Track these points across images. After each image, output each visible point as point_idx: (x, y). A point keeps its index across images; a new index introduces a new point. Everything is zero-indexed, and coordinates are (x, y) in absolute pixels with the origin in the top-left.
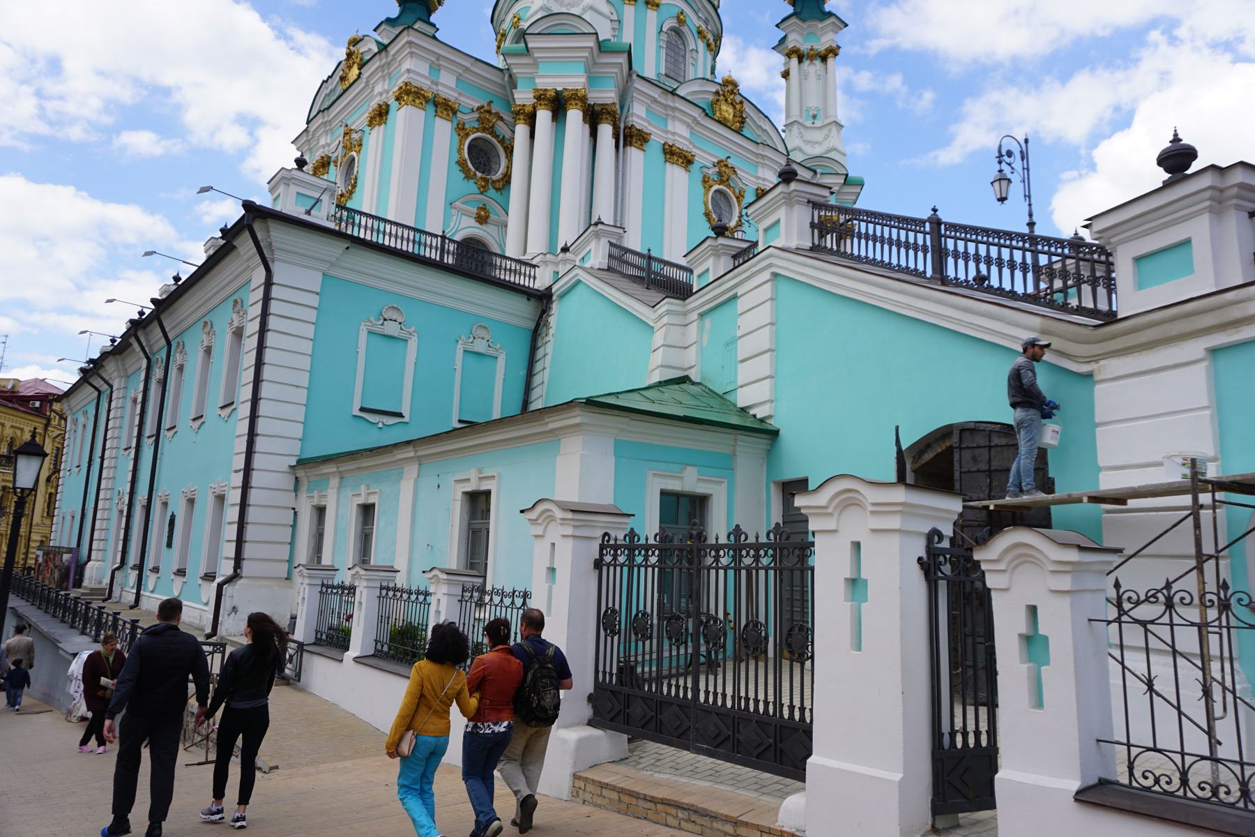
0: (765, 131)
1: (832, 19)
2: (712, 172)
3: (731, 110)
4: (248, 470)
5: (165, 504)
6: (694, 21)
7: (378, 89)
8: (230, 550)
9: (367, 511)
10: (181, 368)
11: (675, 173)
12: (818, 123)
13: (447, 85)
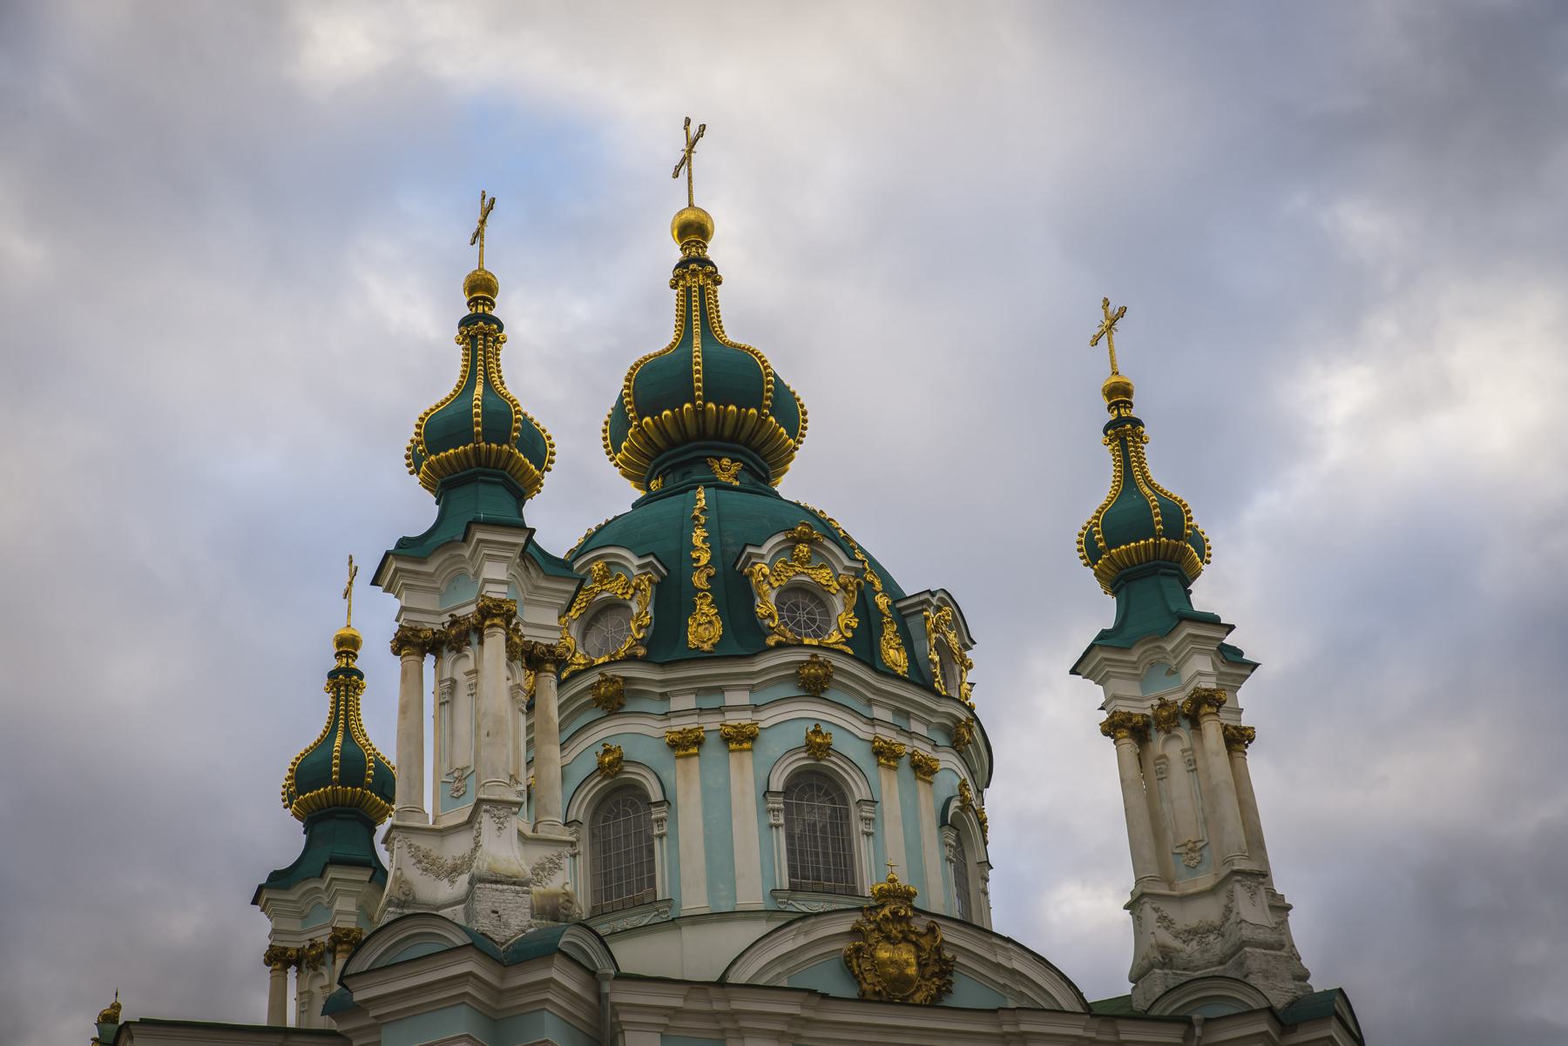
0: (1013, 972)
1: (1188, 629)
3: (906, 954)
6: (850, 734)
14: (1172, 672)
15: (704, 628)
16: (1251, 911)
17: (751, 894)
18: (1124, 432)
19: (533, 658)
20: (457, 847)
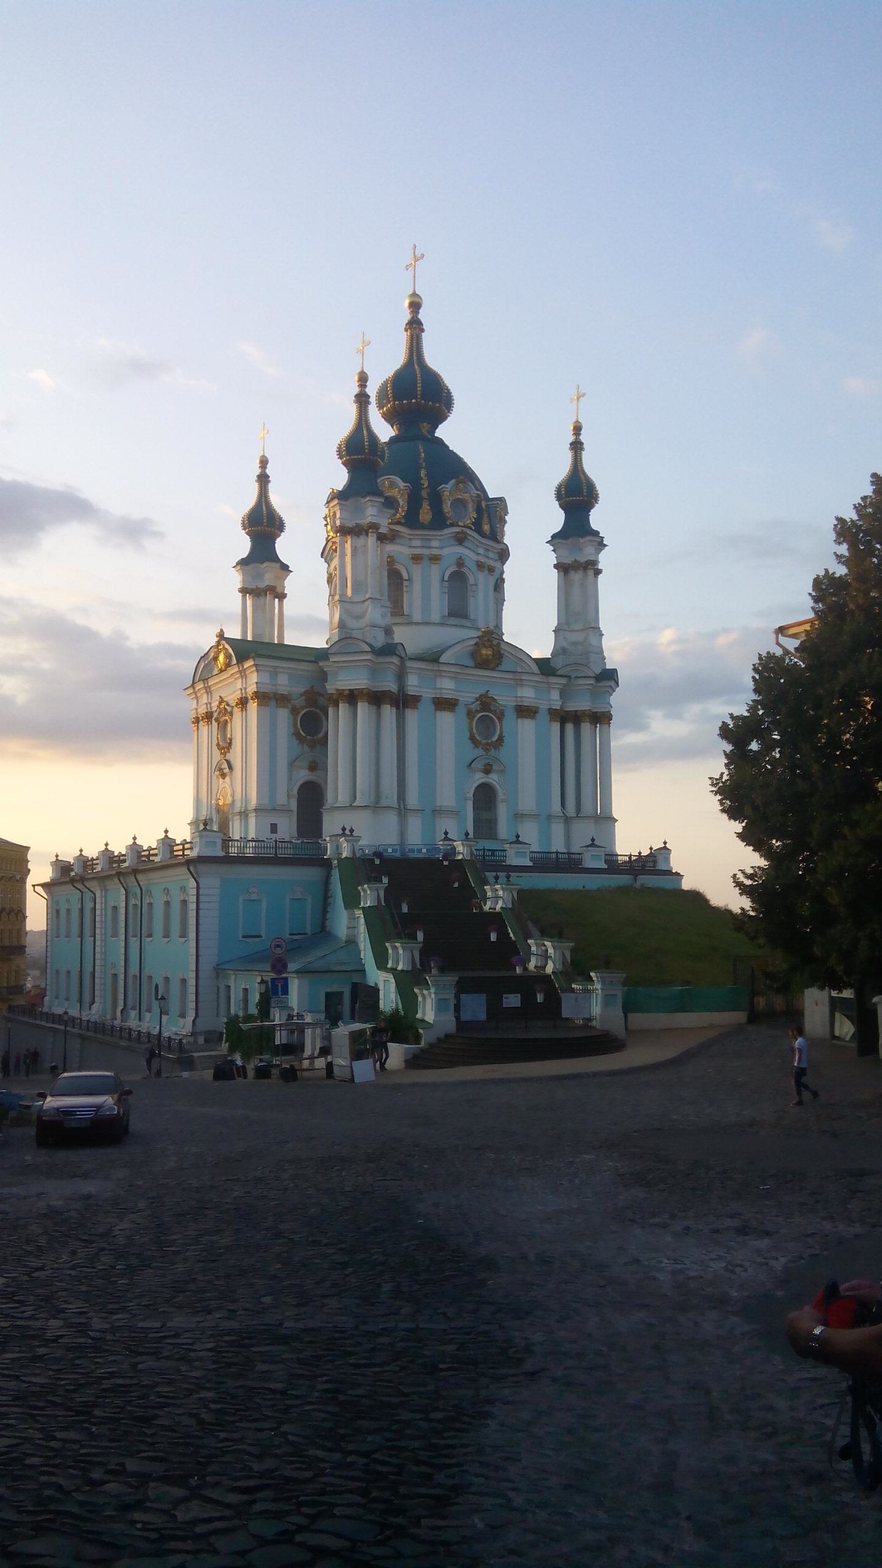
1: (589, 538)
2: (475, 706)
5: (150, 977)
9: (246, 990)
10: (150, 904)
13: (283, 684)
14: (580, 549)
15: (425, 514)
16: (593, 641)
17: (435, 617)
18: (577, 447)
19: (381, 538)
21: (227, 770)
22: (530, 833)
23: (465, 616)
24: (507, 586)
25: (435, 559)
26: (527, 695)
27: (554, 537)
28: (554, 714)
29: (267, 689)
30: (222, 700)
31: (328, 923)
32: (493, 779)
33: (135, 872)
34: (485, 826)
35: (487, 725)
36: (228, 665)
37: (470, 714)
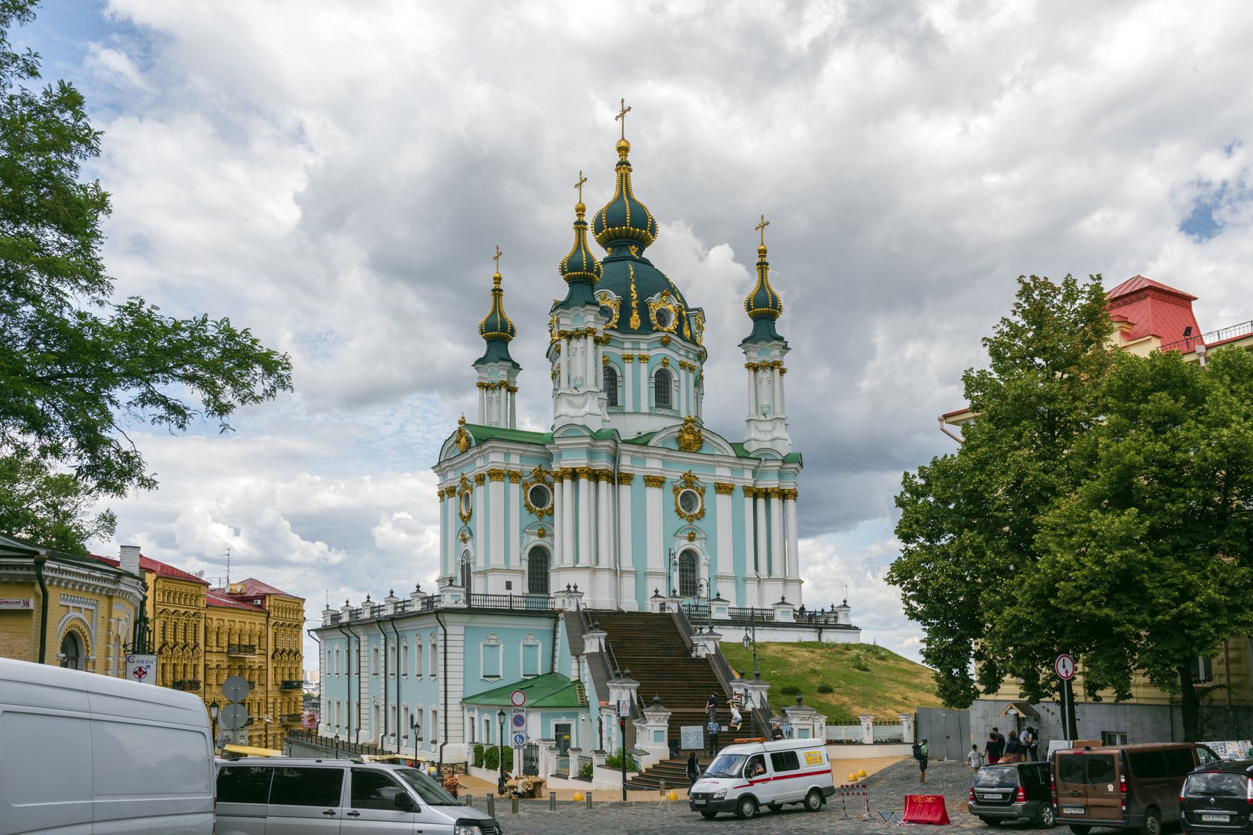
3: (691, 437)
4: (446, 704)
7: (479, 463)
8: (443, 733)
10: (406, 648)
11: (654, 494)
12: (769, 417)
13: (515, 463)
15: (635, 321)
17: (645, 408)
19: (597, 341)
20: (578, 401)
21: (467, 535)
22: (727, 590)
23: (670, 408)
24: (706, 383)
25: (643, 359)
26: (723, 474)
27: (745, 341)
28: (747, 490)
29: (501, 467)
30: (463, 479)
31: (556, 666)
32: (696, 546)
33: (392, 619)
34: (689, 586)
35: (688, 500)
36: (468, 447)
37: (676, 490)
